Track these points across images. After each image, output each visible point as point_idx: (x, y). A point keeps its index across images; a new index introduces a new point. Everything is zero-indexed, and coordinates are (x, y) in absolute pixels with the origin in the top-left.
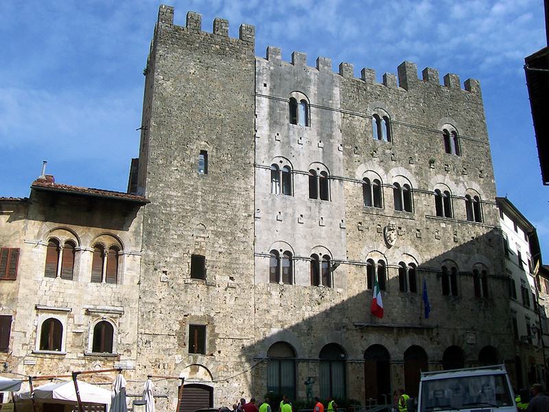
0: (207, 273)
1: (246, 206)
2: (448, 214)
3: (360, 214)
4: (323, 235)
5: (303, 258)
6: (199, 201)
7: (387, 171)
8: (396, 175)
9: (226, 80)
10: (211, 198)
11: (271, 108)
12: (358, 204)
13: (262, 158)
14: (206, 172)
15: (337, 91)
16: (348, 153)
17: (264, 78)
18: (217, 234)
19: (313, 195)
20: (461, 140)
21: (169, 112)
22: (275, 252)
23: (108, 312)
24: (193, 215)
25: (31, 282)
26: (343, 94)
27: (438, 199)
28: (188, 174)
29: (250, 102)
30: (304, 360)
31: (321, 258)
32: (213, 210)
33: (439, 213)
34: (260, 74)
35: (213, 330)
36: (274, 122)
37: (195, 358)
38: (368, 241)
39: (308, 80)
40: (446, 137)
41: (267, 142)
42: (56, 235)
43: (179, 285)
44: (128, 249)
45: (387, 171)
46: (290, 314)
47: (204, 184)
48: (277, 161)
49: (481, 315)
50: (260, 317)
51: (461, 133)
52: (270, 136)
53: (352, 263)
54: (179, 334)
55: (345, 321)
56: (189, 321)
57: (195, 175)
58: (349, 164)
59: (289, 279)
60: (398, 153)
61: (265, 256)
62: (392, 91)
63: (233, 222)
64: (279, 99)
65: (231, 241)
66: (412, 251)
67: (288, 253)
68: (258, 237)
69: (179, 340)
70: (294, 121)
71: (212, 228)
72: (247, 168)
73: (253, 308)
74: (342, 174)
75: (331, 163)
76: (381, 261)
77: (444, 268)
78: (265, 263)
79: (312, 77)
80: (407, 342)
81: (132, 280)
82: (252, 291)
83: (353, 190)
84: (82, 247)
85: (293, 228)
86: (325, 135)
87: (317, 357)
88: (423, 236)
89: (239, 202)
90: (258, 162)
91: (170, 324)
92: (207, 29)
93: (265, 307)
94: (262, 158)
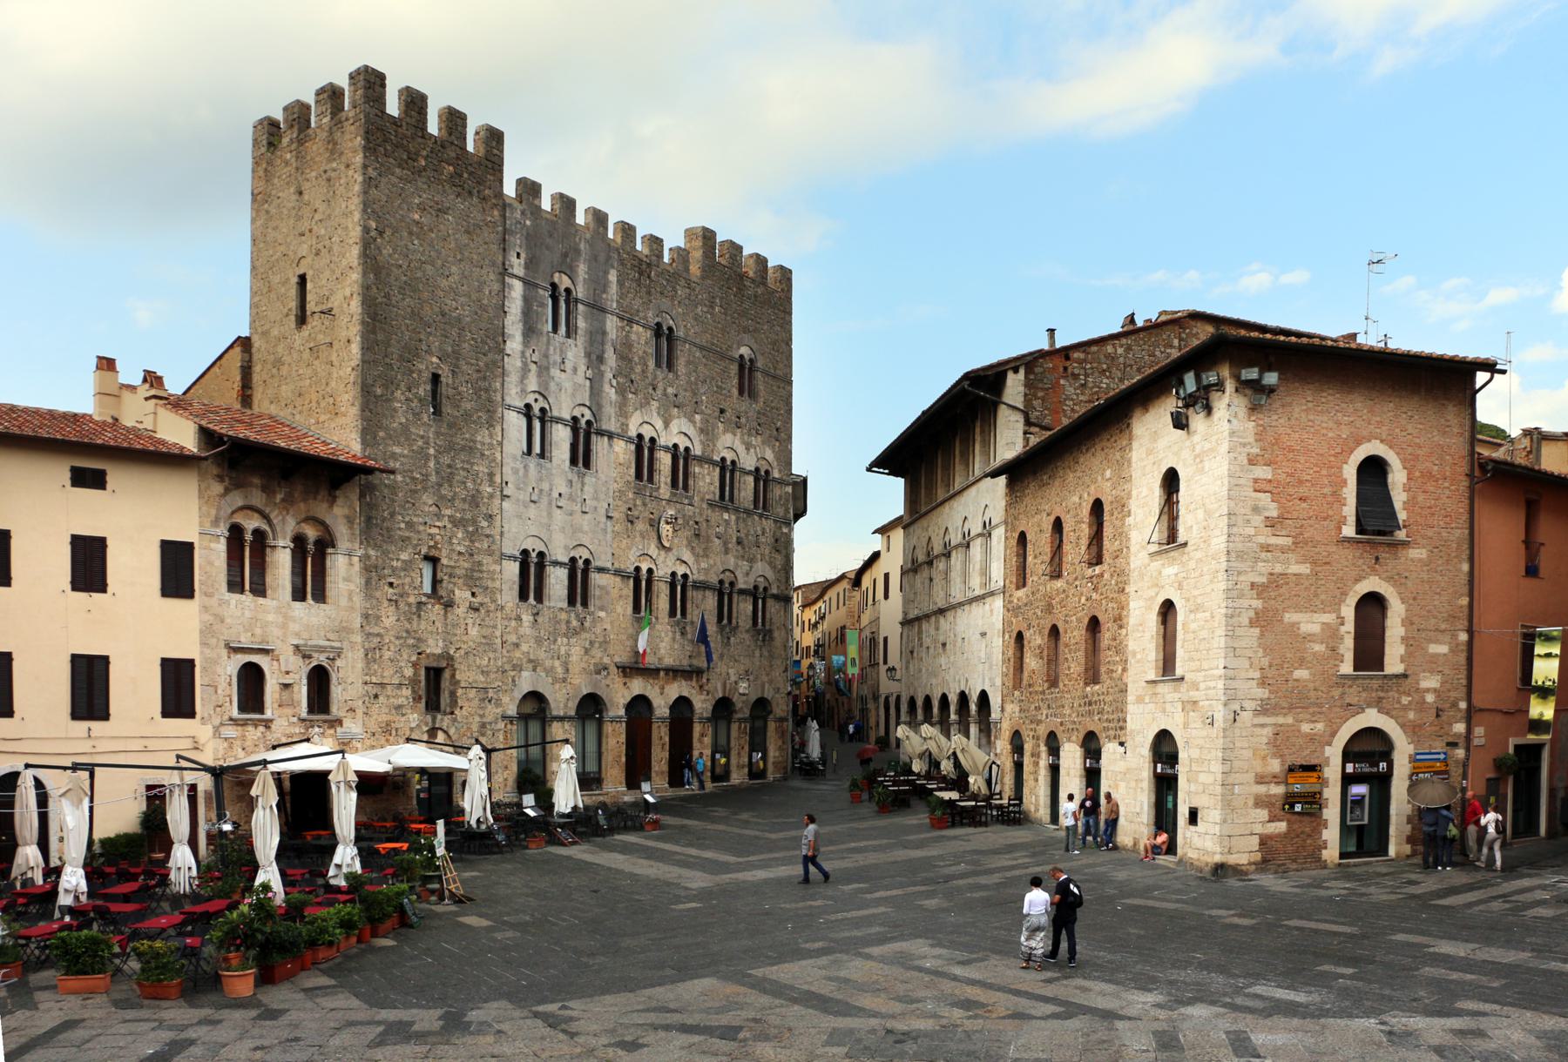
0: (444, 584)
1: (491, 475)
2: (732, 499)
3: (631, 495)
4: (586, 528)
5: (561, 564)
6: (432, 464)
7: (667, 425)
8: (677, 432)
9: (465, 239)
10: (446, 460)
11: (527, 300)
13: (513, 392)
14: (437, 412)
15: (613, 277)
16: (621, 391)
17: (516, 241)
18: (456, 523)
19: (574, 461)
20: (759, 375)
21: (387, 296)
22: (525, 552)
23: (321, 649)
24: (425, 489)
25: (214, 602)
26: (620, 283)
27: (723, 469)
28: (417, 415)
29: (496, 287)
30: (561, 719)
31: (581, 562)
32: (449, 479)
33: (722, 496)
34: (512, 233)
35: (453, 676)
36: (530, 331)
37: (434, 719)
38: (638, 539)
39: (578, 252)
40: (741, 367)
41: (519, 364)
42: (239, 519)
43: (410, 605)
44: (343, 543)
45: (667, 425)
47: (438, 434)
48: (530, 399)
49: (757, 653)
51: (759, 364)
52: (523, 353)
53: (618, 573)
54: (414, 682)
55: (606, 660)
56: (424, 662)
57: (426, 419)
58: (623, 413)
59: (539, 598)
60: (682, 393)
61: (515, 558)
62: (683, 282)
63: (474, 500)
64: (536, 286)
65: (473, 534)
66: (687, 556)
67: (541, 555)
68: (505, 529)
69: (414, 691)
70: (555, 329)
71: (448, 512)
72: (490, 413)
73: (499, 641)
74: (611, 425)
75: (600, 406)
76: (650, 571)
77: (721, 582)
78: (513, 569)
79: (582, 246)
80: (675, 690)
81: (350, 599)
82: (499, 614)
83: (623, 450)
84: (281, 543)
85: (550, 515)
86: (595, 359)
87: (573, 713)
88: (703, 533)
89: (482, 469)
90: (508, 400)
91: (401, 667)
92: (433, 127)
93: (513, 638)
94: (513, 392)
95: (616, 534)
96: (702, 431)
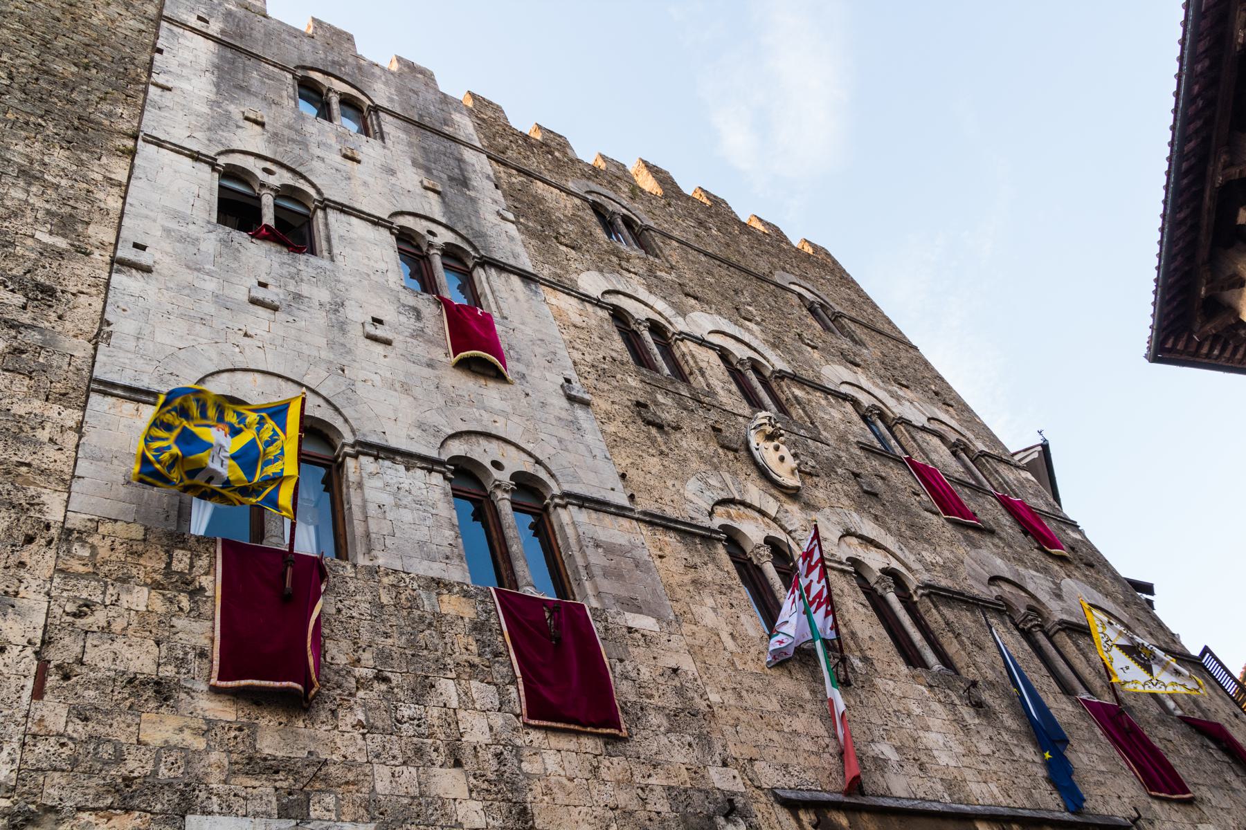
12: (614, 355)
46: (347, 720)
50: (78, 729)
55: (721, 779)
95: (615, 442)
96: (774, 346)
